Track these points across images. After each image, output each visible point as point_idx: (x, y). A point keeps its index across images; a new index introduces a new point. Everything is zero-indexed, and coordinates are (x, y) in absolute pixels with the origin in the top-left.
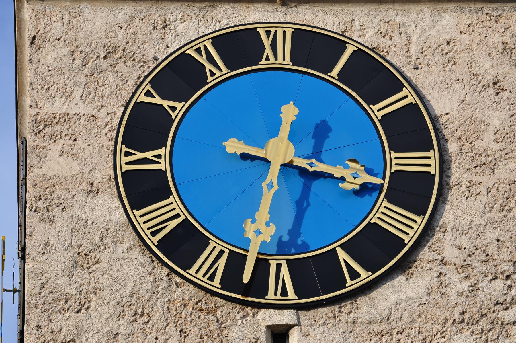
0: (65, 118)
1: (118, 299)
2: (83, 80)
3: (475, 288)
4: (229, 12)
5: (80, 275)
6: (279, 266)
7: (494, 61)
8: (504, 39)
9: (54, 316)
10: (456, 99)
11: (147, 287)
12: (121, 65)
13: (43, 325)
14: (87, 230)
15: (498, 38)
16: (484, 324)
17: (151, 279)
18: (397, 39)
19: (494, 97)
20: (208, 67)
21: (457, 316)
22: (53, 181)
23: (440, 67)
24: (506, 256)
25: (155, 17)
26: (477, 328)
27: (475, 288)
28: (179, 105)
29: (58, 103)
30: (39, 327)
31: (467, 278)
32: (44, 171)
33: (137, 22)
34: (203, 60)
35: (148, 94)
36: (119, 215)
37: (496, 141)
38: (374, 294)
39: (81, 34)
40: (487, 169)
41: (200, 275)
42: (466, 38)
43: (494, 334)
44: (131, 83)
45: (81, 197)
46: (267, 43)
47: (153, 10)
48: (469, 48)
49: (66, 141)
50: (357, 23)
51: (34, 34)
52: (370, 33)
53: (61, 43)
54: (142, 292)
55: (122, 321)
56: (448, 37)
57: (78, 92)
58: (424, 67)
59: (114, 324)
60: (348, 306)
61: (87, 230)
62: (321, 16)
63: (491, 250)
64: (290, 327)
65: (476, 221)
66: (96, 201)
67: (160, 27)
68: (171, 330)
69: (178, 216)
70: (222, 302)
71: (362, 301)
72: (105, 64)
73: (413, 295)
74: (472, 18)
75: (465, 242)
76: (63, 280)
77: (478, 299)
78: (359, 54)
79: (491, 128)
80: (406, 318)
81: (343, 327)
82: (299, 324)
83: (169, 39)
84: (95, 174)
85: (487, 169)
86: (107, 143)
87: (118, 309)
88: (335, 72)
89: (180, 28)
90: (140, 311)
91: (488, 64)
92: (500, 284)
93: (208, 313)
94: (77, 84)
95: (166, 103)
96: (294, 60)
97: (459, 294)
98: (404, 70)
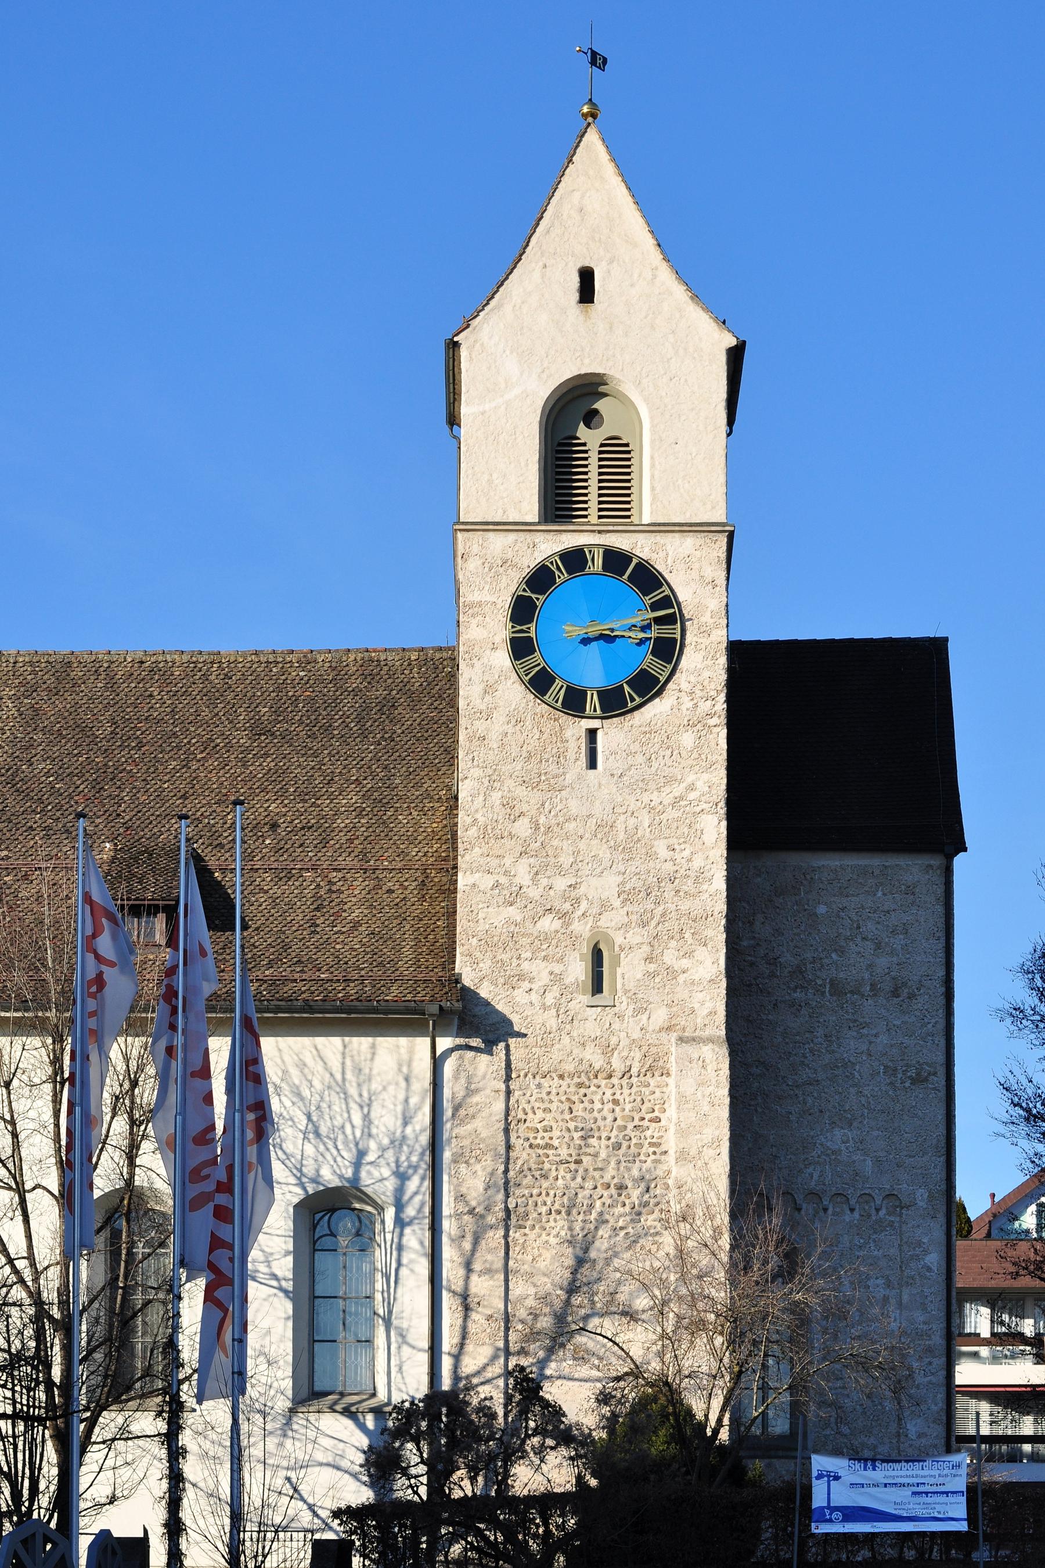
0: (480, 604)
3: (696, 705)
5: (488, 698)
10: (691, 592)
15: (715, 554)
18: (662, 555)
20: (557, 573)
21: (686, 722)
27: (696, 705)
28: (540, 597)
29: (476, 593)
33: (519, 544)
34: (554, 568)
35: (524, 590)
38: (643, 710)
43: (704, 732)
44: (515, 581)
45: (488, 652)
49: (480, 618)
50: (639, 544)
52: (646, 550)
56: (687, 553)
57: (487, 588)
58: (675, 571)
59: (505, 727)
60: (628, 716)
65: (699, 666)
68: (535, 730)
69: (539, 664)
71: (636, 713)
72: (501, 570)
74: (702, 542)
75: (692, 679)
76: (479, 701)
78: (639, 565)
79: (709, 609)
80: (659, 724)
81: (626, 729)
83: (536, 554)
85: (706, 635)
87: (508, 719)
88: (626, 576)
89: (543, 547)
92: (709, 703)
95: (534, 596)
98: (664, 573)
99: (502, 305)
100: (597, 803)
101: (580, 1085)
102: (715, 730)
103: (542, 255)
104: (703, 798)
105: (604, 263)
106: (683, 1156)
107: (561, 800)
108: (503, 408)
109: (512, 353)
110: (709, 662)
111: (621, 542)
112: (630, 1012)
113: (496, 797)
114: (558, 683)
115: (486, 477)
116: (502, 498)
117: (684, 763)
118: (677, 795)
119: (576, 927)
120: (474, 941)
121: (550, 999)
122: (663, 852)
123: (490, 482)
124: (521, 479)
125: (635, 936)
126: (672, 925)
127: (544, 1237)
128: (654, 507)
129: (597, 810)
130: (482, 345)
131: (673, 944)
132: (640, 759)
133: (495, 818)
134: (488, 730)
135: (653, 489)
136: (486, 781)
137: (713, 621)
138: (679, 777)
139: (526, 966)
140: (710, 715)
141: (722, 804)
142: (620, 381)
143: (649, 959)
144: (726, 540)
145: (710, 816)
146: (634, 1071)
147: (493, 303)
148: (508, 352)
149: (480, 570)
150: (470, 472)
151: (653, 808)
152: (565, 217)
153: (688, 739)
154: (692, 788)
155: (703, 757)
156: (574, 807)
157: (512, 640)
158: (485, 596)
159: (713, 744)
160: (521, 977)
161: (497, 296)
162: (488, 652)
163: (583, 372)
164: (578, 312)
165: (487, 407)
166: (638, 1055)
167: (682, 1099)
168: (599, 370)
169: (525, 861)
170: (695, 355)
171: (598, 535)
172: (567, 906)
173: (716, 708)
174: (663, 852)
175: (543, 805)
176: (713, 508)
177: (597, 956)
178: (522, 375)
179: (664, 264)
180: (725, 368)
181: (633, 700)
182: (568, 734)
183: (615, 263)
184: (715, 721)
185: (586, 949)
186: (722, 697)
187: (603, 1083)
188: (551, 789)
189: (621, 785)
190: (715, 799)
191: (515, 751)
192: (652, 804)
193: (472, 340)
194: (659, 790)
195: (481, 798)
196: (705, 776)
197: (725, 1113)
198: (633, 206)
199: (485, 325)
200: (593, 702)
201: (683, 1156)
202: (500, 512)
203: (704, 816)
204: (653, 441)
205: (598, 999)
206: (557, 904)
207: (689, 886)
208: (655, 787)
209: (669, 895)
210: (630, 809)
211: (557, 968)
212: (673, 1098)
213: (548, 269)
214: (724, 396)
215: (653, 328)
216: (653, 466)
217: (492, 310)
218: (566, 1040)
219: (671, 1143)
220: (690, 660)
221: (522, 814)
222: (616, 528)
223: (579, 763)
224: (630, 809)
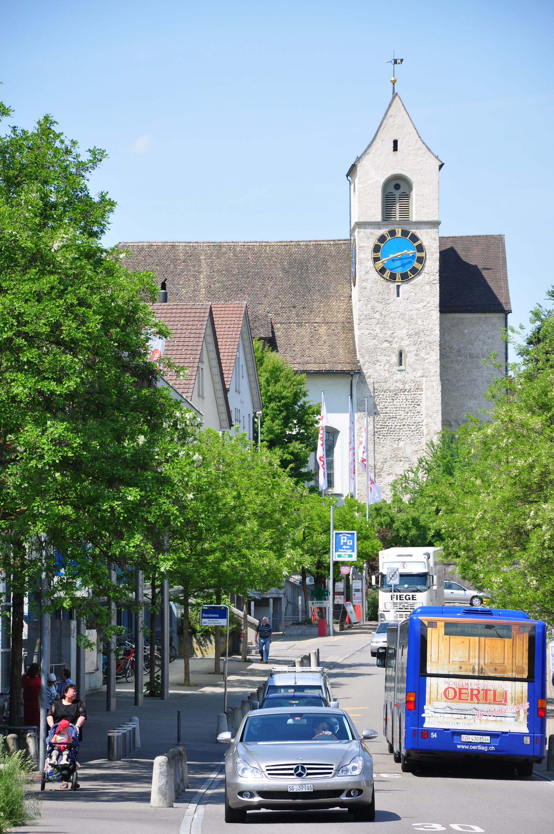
5: (366, 276)
36: (372, 265)
101: (396, 394)
106: (428, 415)
111: (407, 228)
112: (410, 372)
113: (369, 306)
119: (394, 346)
120: (363, 350)
121: (386, 368)
122: (420, 322)
125: (412, 348)
126: (423, 344)
127: (385, 441)
131: (423, 350)
132: (413, 294)
139: (379, 358)
141: (438, 308)
143: (416, 355)
146: (412, 390)
153: (427, 287)
154: (429, 302)
156: (393, 308)
157: (374, 258)
158: (365, 244)
160: (378, 361)
166: (413, 384)
167: (427, 398)
169: (378, 325)
172: (391, 339)
174: (420, 322)
177: (401, 354)
181: (411, 276)
184: (435, 282)
185: (397, 353)
186: (438, 274)
187: (402, 393)
190: (436, 306)
196: (433, 299)
197: (440, 402)
200: (398, 277)
201: (428, 415)
205: (402, 368)
206: (388, 339)
207: (428, 333)
209: (422, 335)
211: (388, 358)
212: (424, 398)
218: (391, 381)
219: (423, 410)
220: (428, 263)
221: (377, 311)
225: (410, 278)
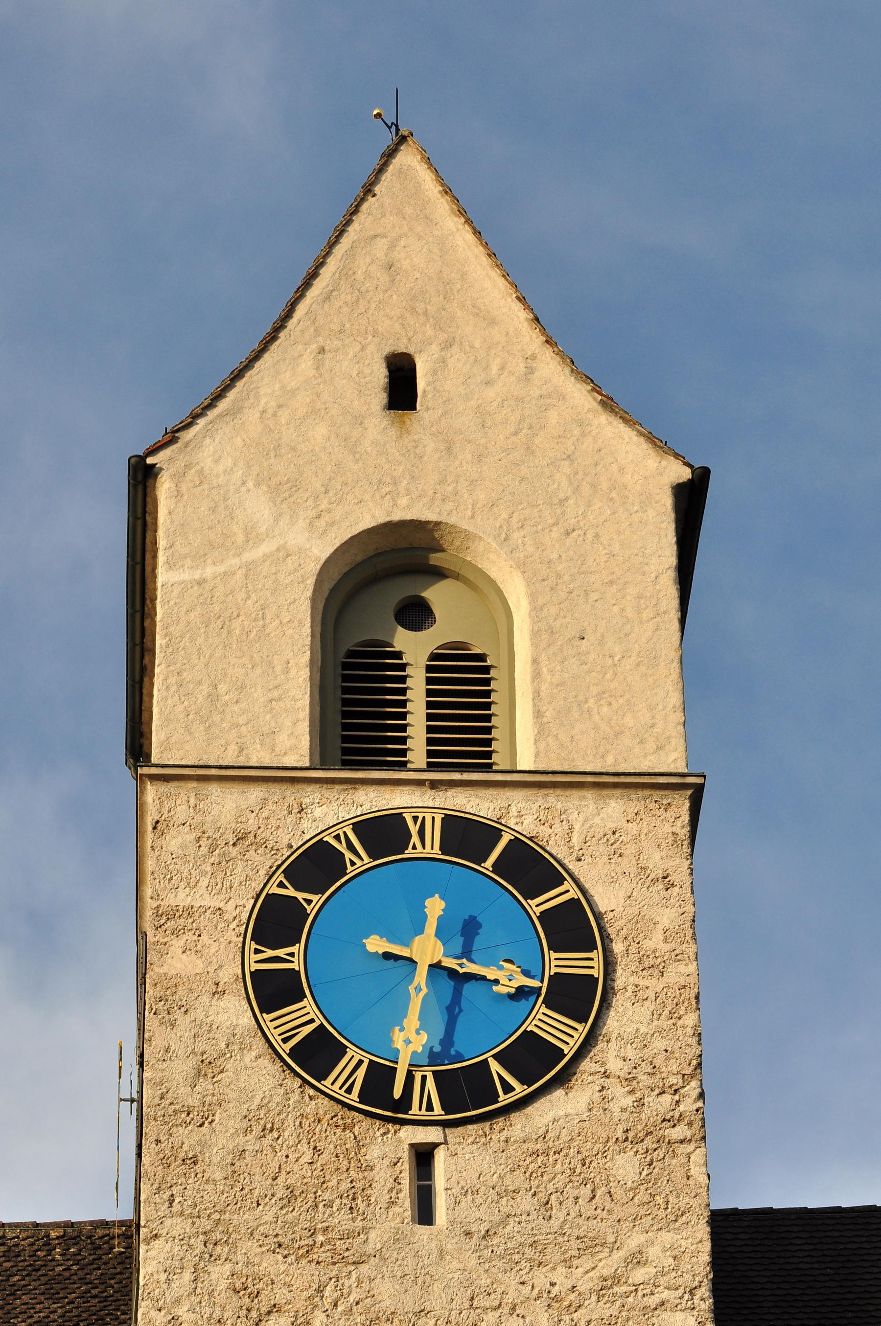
0: (189, 911)
1: (245, 1113)
2: (209, 868)
4: (372, 795)
5: (204, 1085)
6: (424, 1078)
7: (664, 854)
8: (674, 829)
9: (174, 1130)
10: (622, 894)
11: (277, 1099)
12: (252, 852)
13: (162, 1139)
14: (211, 1035)
15: (667, 828)
16: (649, 1142)
17: (282, 1091)
18: (558, 828)
19: (663, 893)
20: (348, 855)
21: (620, 1134)
22: (174, 981)
23: (605, 859)
24: (674, 1068)
25: (290, 800)
26: (641, 1148)
28: (314, 898)
29: (182, 894)
30: (158, 1141)
31: (632, 1092)
32: (165, 969)
33: (270, 806)
34: (342, 848)
35: (281, 885)
36: (247, 1019)
37: (665, 941)
38: (529, 1110)
39: (209, 819)
40: (656, 973)
41: (336, 1087)
42: (633, 828)
43: (661, 1153)
44: (262, 872)
45: (205, 999)
46: (414, 829)
47: (288, 793)
48: (637, 838)
49: (190, 937)
50: (514, 810)
51: (156, 818)
53: (186, 828)
54: (272, 1105)
55: (249, 1137)
56: (612, 826)
57: (204, 882)
59: (241, 1140)
60: (500, 1122)
61: (211, 1035)
62: (475, 801)
63: (658, 1062)
64: (436, 1145)
65: (643, 1029)
66: (221, 1004)
67: (295, 811)
68: (303, 1147)
69: (312, 1021)
70: (361, 1117)
71: (516, 1118)
72: (234, 851)
73: (573, 1112)
74: (640, 806)
75: (630, 1053)
76: (184, 1090)
77: (643, 1116)
78: (515, 843)
79: (660, 927)
80: (565, 1137)
81: (494, 1145)
82: (446, 1142)
83: (305, 824)
84: (221, 974)
85: (656, 973)
86: (235, 939)
87: (245, 1124)
89: (318, 812)
90: (269, 1126)
91: (657, 856)
92: (667, 1099)
93: (344, 1130)
94: (203, 873)
95: (300, 896)
96: (444, 849)
97: (623, 1110)
98: (566, 861)
99: (240, 410)
100: (437, 1287)
102: (682, 1149)
103: (317, 332)
104: (662, 1281)
105: (434, 348)
107: (359, 1282)
108: (240, 574)
109: (258, 485)
110: (666, 1023)
114: (353, 1054)
115: (205, 689)
116: (238, 726)
117: (619, 1212)
118: (606, 1272)
123: (214, 698)
124: (275, 694)
128: (542, 745)
129: (437, 1301)
130: (201, 472)
133: (217, 1315)
134: (202, 1144)
135: (538, 714)
136: (198, 1244)
137: (667, 947)
138: (611, 1239)
140: (672, 1121)
141: (704, 1291)
142: (468, 536)
144: (687, 804)
145: (679, 1316)
147: (223, 405)
148: (250, 484)
149: (191, 850)
150: (172, 680)
151: (556, 1299)
152: (359, 275)
154: (637, 1259)
155: (660, 1200)
158: (203, 898)
159: (679, 1175)
161: (232, 395)
162: (205, 999)
163: (396, 517)
164: (385, 423)
165: (209, 571)
168: (429, 515)
170: (614, 495)
171: (430, 793)
173: (682, 1108)
175: (320, 1291)
176: (659, 748)
178: (276, 521)
179: (548, 352)
180: (673, 516)
182: (373, 1153)
183: (455, 349)
184: (680, 1132)
188: (338, 1259)
189: (487, 1253)
191: (261, 1184)
192: (555, 1290)
193: (181, 464)
194: (568, 1263)
195: (187, 1276)
196: (666, 1237)
198: (485, 261)
199: (208, 441)
202: (232, 750)
203: (665, 1315)
204: (535, 634)
208: (558, 1257)
210: (509, 1299)
213: (328, 355)
214: (673, 561)
215: (529, 450)
216: (536, 675)
217: (221, 416)
221: (275, 1309)
222: (466, 776)
223: (397, 1209)
224: (509, 1299)
225: (504, 1099)
